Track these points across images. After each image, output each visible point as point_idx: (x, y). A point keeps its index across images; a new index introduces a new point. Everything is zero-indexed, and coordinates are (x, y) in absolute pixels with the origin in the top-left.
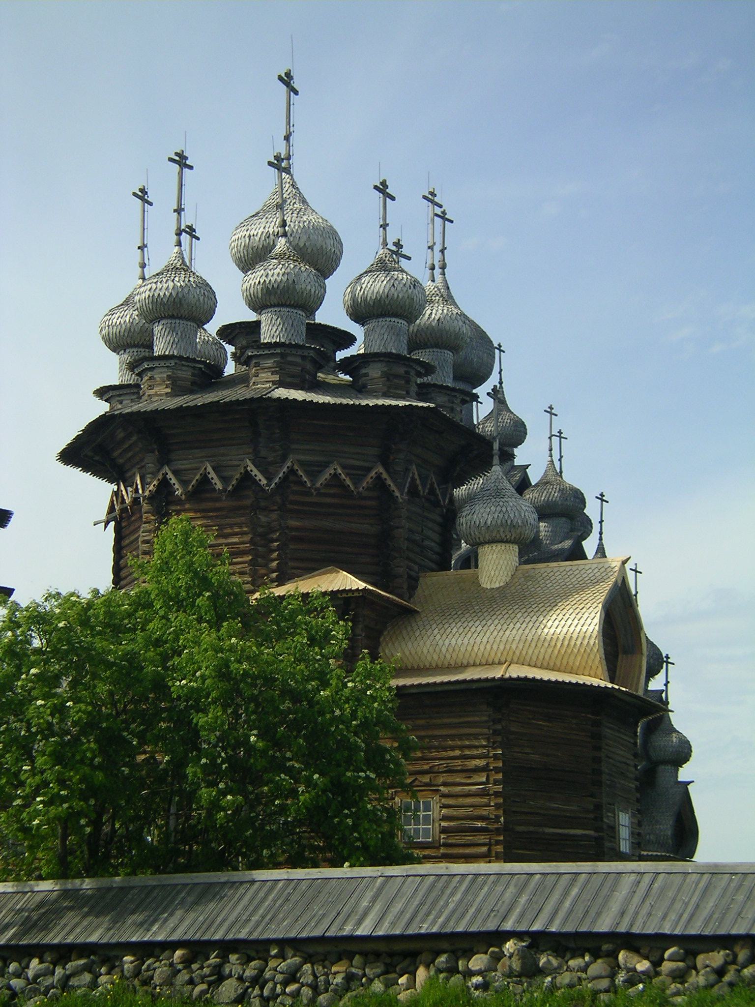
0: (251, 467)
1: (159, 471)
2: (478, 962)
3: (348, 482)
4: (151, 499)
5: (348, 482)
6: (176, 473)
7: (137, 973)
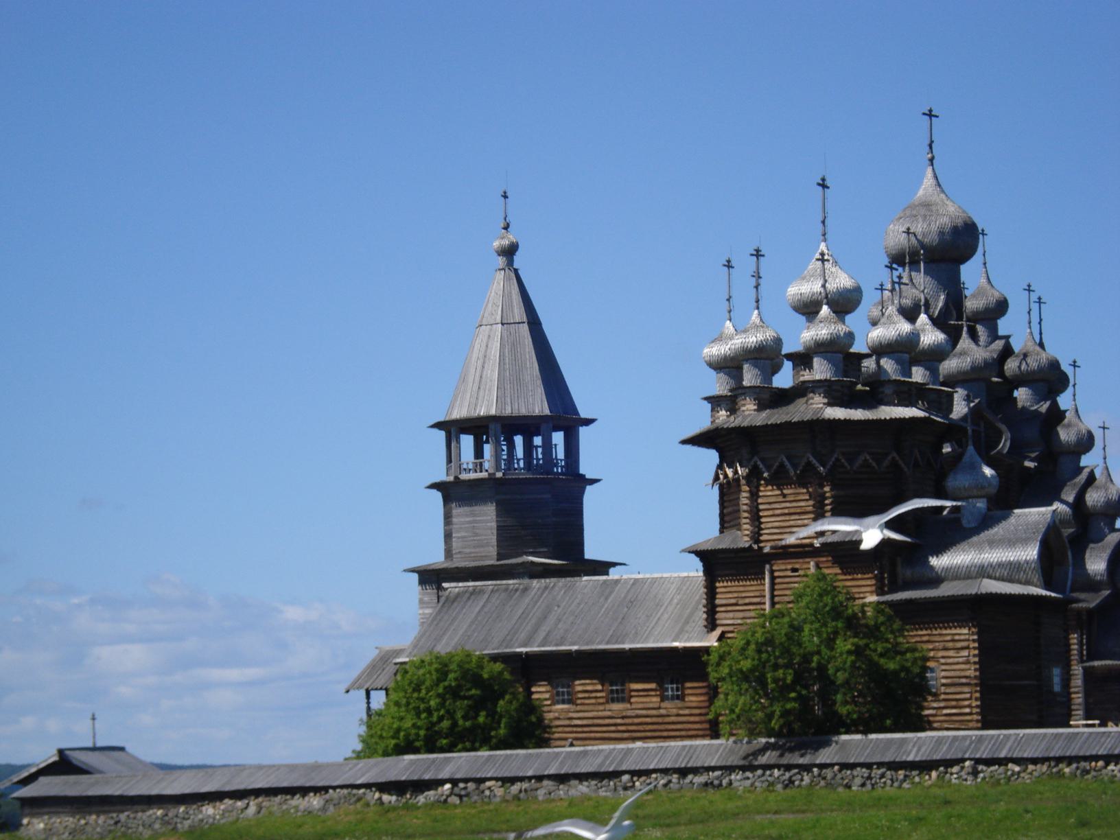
0: (812, 459)
1: (750, 460)
2: (955, 769)
3: (874, 464)
4: (748, 478)
5: (874, 464)
6: (763, 460)
7: (819, 775)
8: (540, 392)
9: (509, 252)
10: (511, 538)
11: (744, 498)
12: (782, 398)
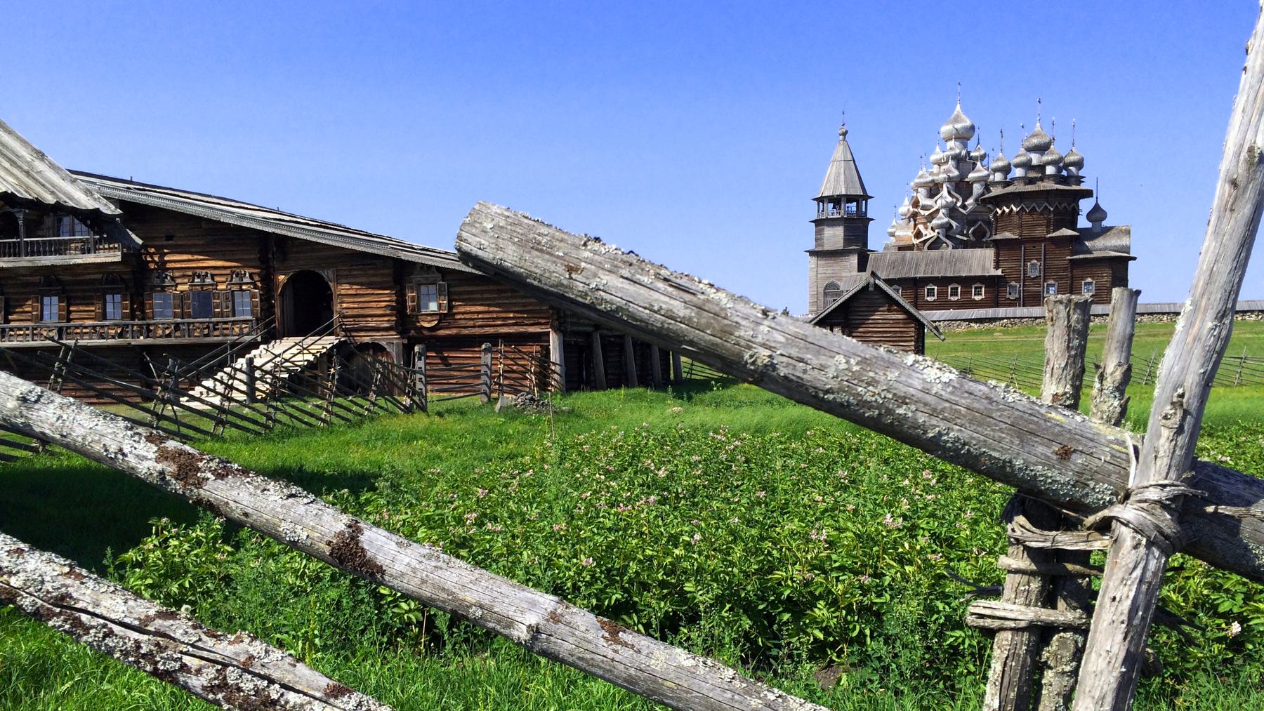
8: (859, 185)
9: (844, 134)
10: (847, 240)
11: (1016, 219)
12: (1031, 181)
